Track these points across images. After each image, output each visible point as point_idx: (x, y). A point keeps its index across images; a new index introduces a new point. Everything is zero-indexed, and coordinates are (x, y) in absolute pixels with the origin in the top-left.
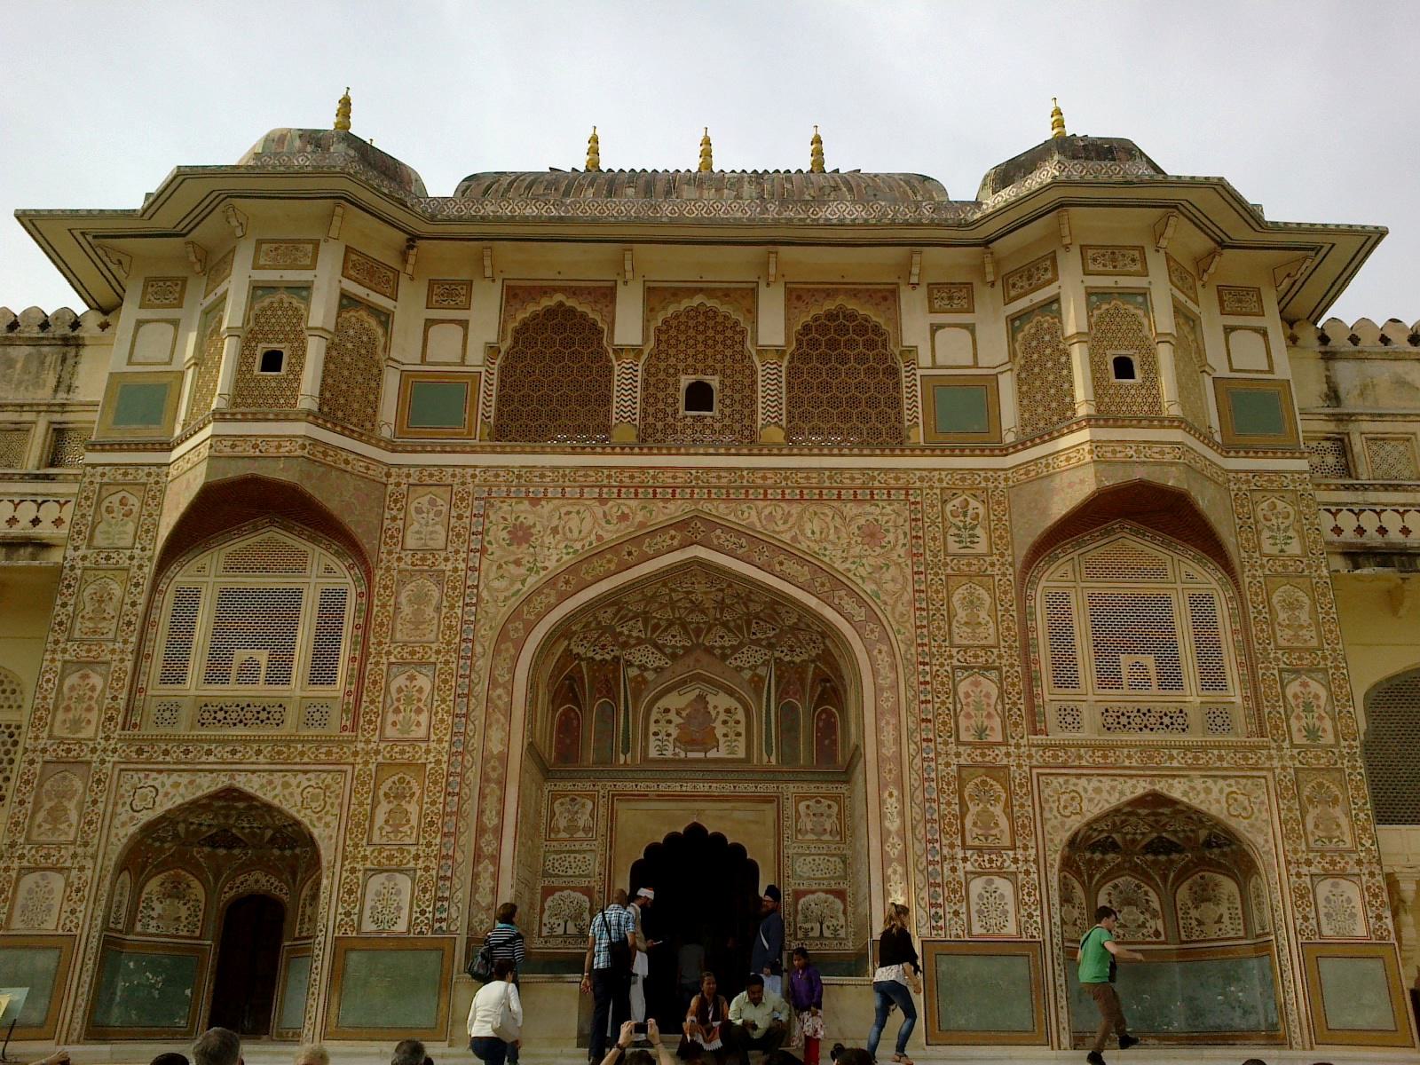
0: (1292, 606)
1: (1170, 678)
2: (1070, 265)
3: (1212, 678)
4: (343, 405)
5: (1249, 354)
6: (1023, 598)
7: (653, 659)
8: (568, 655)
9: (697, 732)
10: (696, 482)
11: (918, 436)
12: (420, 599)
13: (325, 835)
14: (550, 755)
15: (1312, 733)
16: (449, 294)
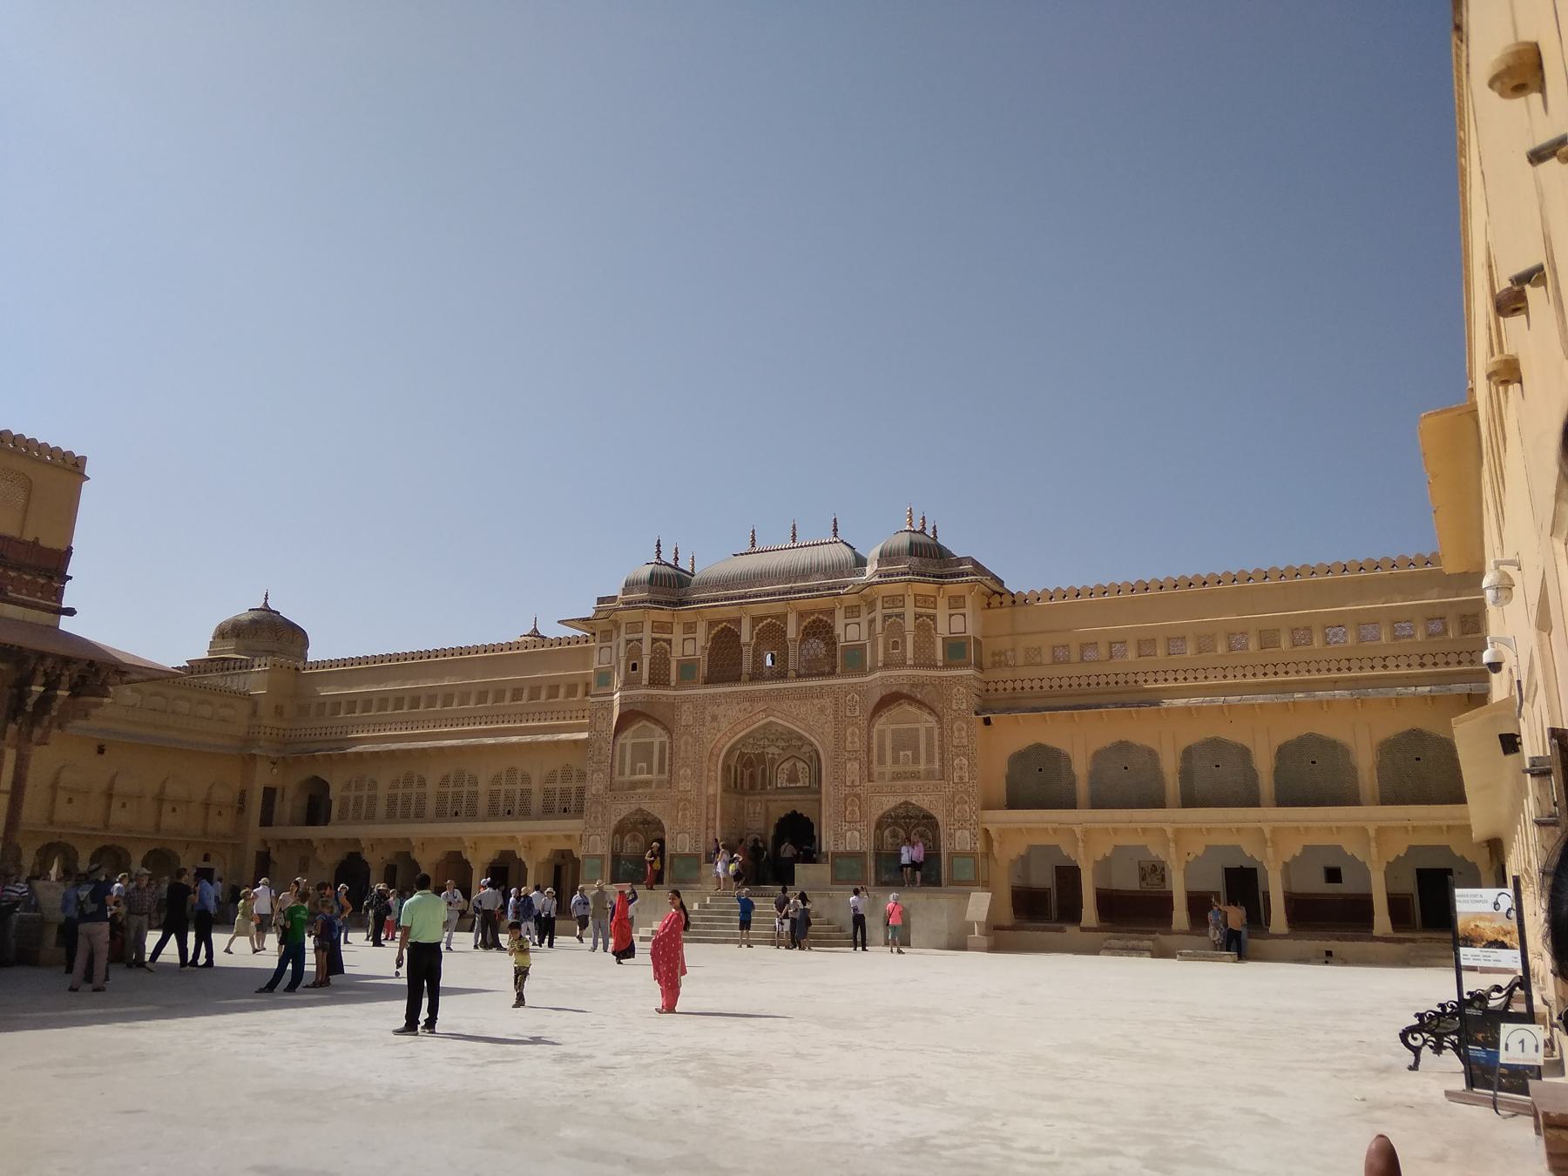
0: (960, 730)
1: (916, 760)
2: (879, 603)
3: (930, 760)
4: (659, 679)
5: (958, 625)
6: (869, 732)
7: (777, 751)
8: (742, 755)
9: (793, 777)
10: (768, 693)
11: (838, 670)
12: (686, 743)
13: (666, 823)
14: (746, 786)
15: (961, 778)
16: (690, 627)
